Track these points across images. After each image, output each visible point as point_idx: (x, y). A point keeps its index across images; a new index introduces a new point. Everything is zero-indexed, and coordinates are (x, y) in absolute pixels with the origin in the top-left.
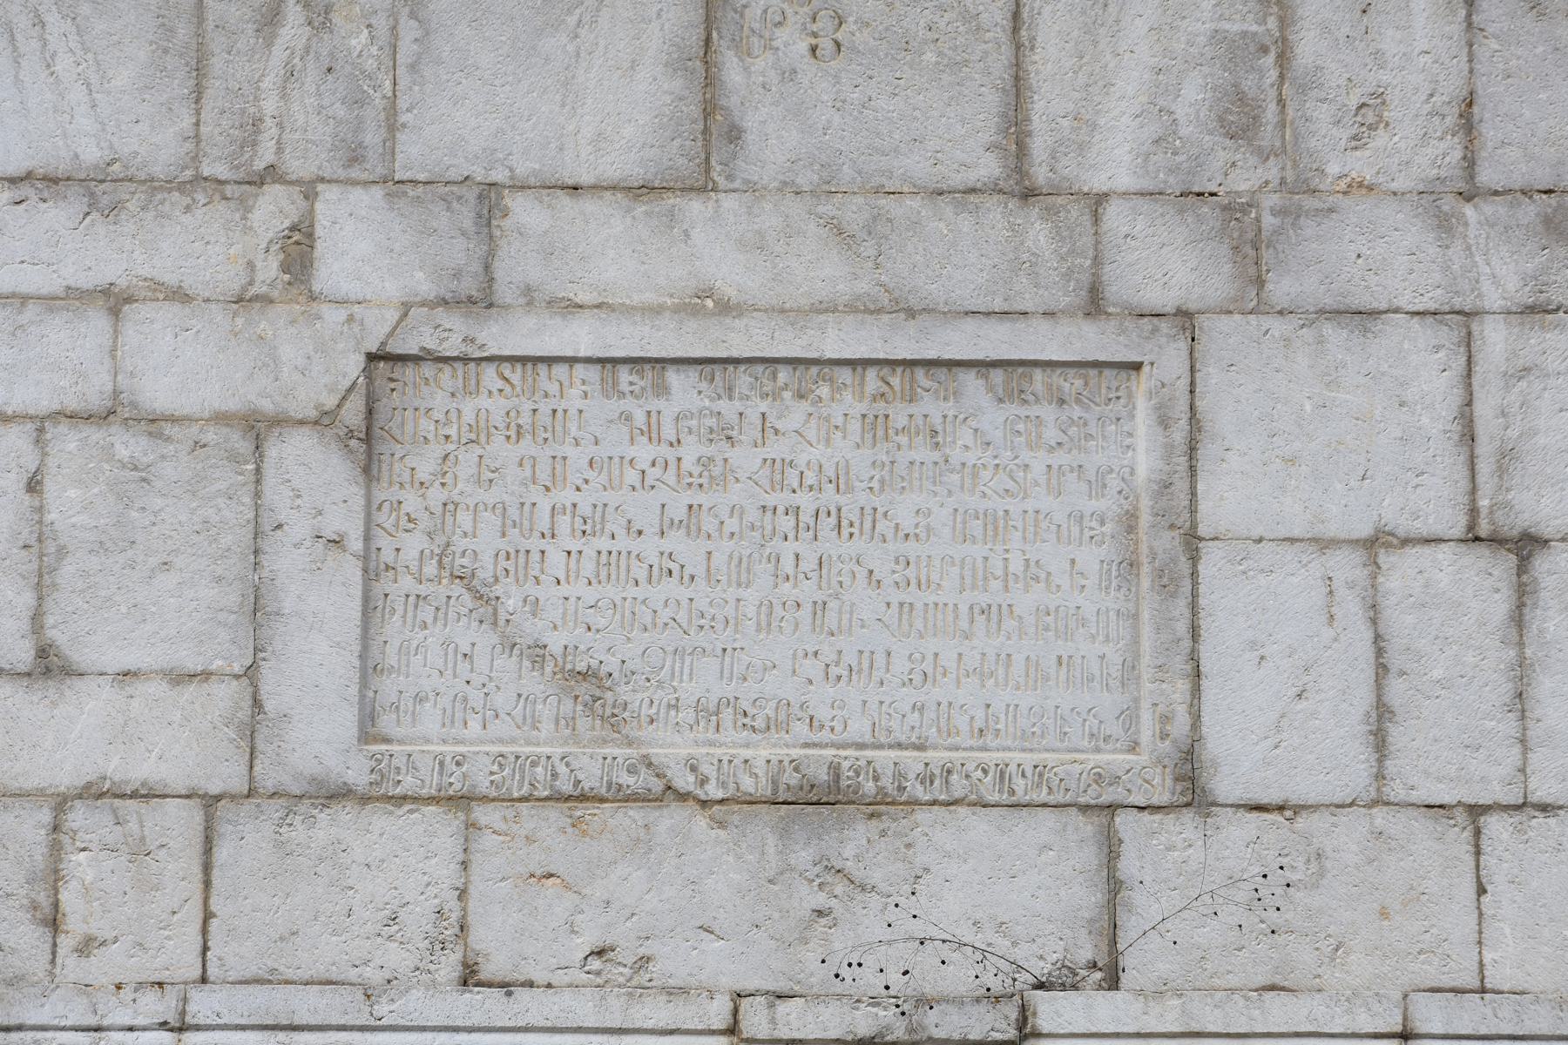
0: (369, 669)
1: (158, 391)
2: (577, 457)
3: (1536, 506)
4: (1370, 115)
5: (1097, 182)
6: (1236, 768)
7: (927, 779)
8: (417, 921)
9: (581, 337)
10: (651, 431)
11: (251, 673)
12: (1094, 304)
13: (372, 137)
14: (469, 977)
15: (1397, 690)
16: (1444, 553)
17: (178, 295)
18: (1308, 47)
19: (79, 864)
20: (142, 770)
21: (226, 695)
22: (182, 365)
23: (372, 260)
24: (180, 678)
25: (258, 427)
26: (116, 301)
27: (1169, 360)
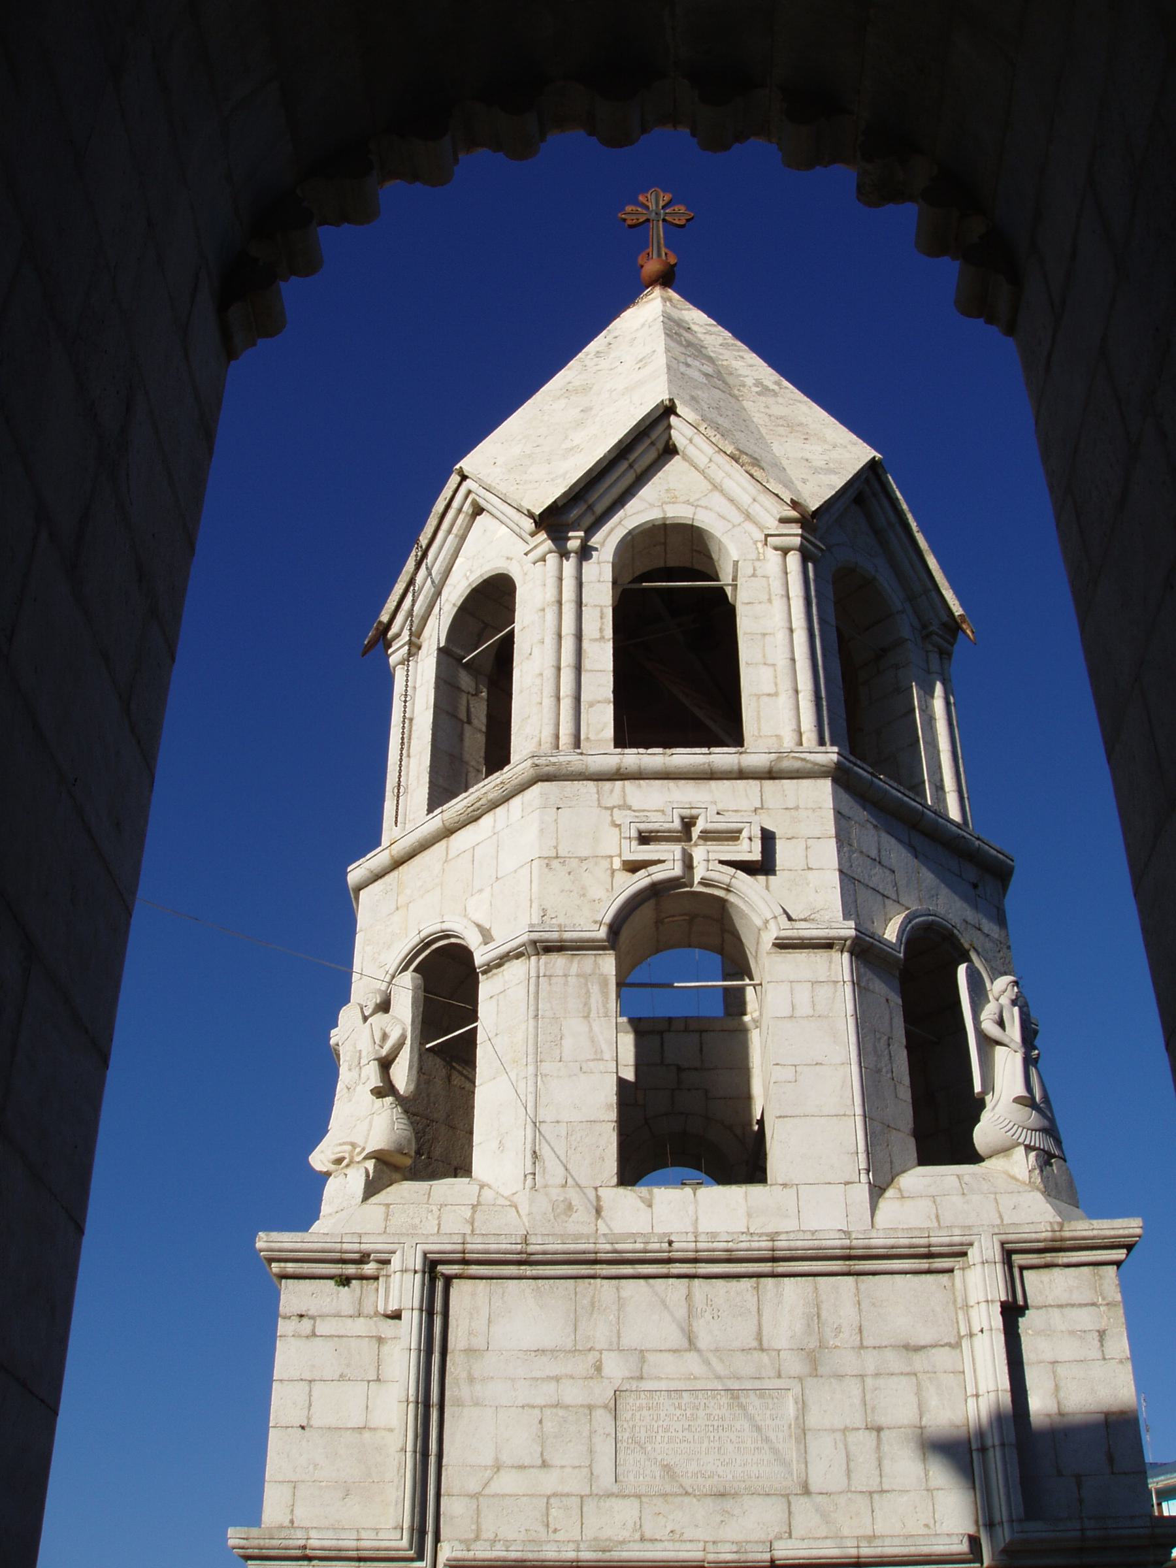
1: (568, 1400)
2: (663, 1414)
3: (882, 1420)
4: (838, 1330)
9: (663, 1385)
10: (680, 1407)
11: (590, 1466)
12: (779, 1376)
13: (615, 1340)
14: (642, 1539)
17: (572, 1377)
18: (824, 1314)
19: (553, 1512)
20: (566, 1490)
21: (586, 1471)
22: (573, 1394)
23: (616, 1369)
24: (575, 1467)
25: (590, 1408)
26: (557, 1379)
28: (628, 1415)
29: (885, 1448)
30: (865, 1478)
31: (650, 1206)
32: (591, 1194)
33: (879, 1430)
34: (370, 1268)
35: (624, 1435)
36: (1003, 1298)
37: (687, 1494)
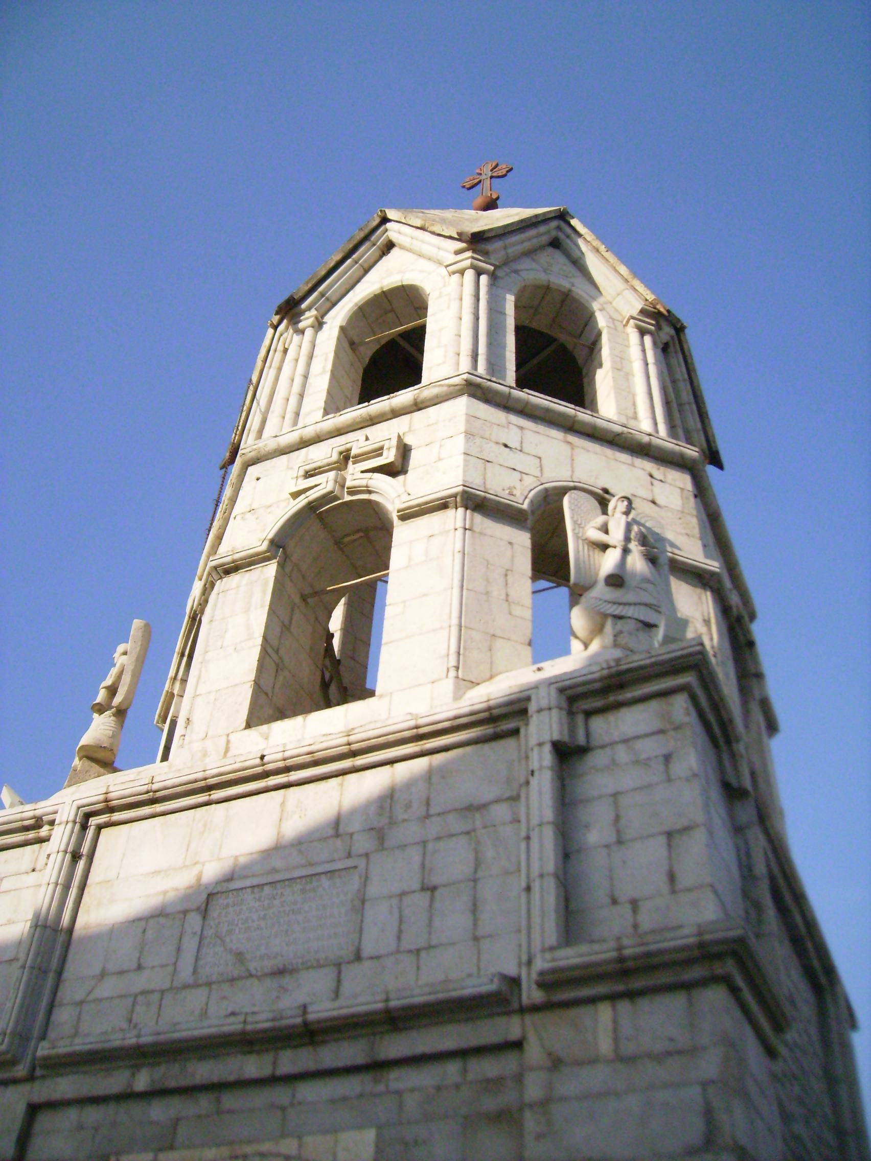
0: (197, 959)
2: (244, 908)
3: (435, 880)
4: (408, 806)
5: (351, 831)
6: (368, 949)
7: (303, 963)
8: (197, 1013)
9: (248, 883)
10: (259, 900)
11: (175, 964)
12: (349, 855)
15: (404, 926)
16: (417, 895)
19: (138, 1009)
27: (362, 863)
28: (215, 915)
29: (437, 904)
30: (414, 937)
31: (267, 738)
32: (224, 739)
33: (433, 889)
34: (44, 831)
35: (209, 932)
36: (556, 737)
37: (251, 976)
